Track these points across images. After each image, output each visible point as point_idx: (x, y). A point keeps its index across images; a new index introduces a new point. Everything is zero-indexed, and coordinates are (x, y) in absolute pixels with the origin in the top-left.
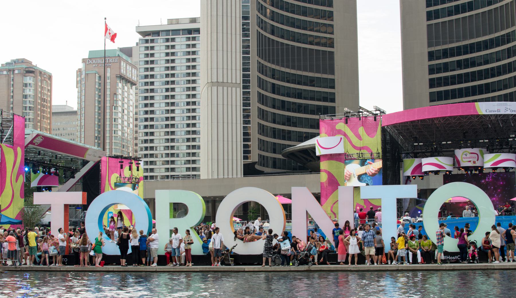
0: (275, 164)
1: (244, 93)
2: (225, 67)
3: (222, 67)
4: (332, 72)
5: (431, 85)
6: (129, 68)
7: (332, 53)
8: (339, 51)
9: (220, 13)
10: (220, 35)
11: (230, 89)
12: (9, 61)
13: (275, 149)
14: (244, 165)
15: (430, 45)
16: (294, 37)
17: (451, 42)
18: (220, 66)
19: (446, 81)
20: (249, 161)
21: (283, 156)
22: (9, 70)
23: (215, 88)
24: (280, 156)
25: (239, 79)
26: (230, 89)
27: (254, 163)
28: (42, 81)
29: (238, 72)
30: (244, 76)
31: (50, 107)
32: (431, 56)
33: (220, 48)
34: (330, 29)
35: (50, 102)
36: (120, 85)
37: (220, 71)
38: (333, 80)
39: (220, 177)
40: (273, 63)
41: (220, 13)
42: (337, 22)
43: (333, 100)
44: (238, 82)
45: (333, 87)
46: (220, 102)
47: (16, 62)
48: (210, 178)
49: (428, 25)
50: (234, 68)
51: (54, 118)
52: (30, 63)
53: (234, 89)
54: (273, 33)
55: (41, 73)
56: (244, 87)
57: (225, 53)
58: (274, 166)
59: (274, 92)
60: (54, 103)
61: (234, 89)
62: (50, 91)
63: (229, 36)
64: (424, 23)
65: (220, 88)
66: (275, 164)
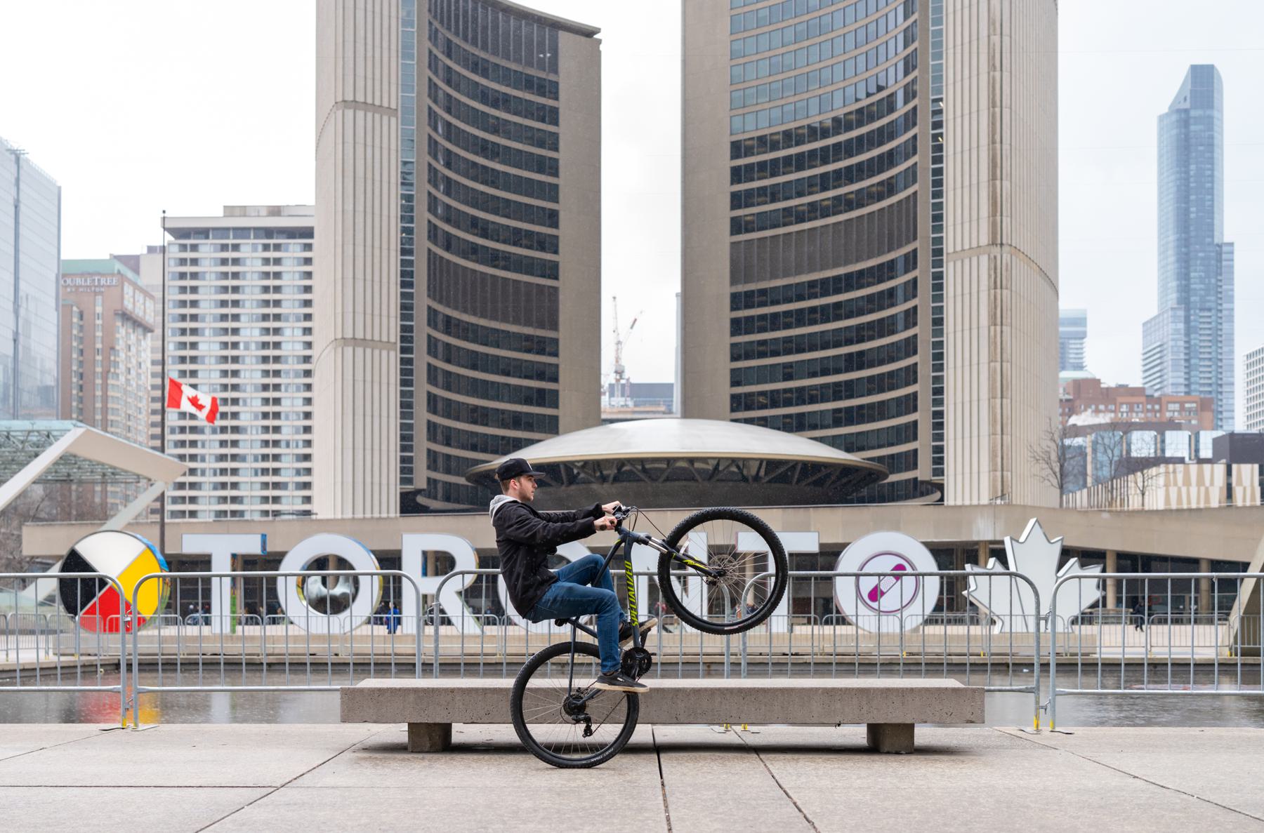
0: (451, 494)
1: (403, 361)
2: (369, 311)
4: (554, 326)
5: (734, 358)
6: (140, 297)
7: (556, 289)
8: (567, 285)
9: (360, 208)
10: (360, 250)
11: (377, 352)
13: (450, 465)
14: (401, 494)
15: (734, 282)
16: (494, 259)
17: (774, 276)
18: (360, 309)
19: (763, 350)
20: (409, 488)
21: (468, 479)
23: (349, 350)
24: (462, 481)
25: (395, 336)
26: (377, 352)
27: (419, 492)
29: (393, 320)
30: (405, 329)
32: (737, 301)
33: (360, 275)
34: (551, 244)
36: (122, 331)
37: (360, 319)
38: (555, 342)
39: (345, 516)
40: (448, 305)
41: (360, 208)
42: (565, 232)
43: (555, 379)
45: (555, 354)
46: (359, 377)
48: (339, 516)
49: (733, 244)
53: (384, 353)
54: (448, 248)
56: (403, 350)
58: (447, 499)
59: (448, 361)
61: (384, 353)
63: (377, 252)
64: (726, 239)
65: (360, 351)
66: (451, 494)
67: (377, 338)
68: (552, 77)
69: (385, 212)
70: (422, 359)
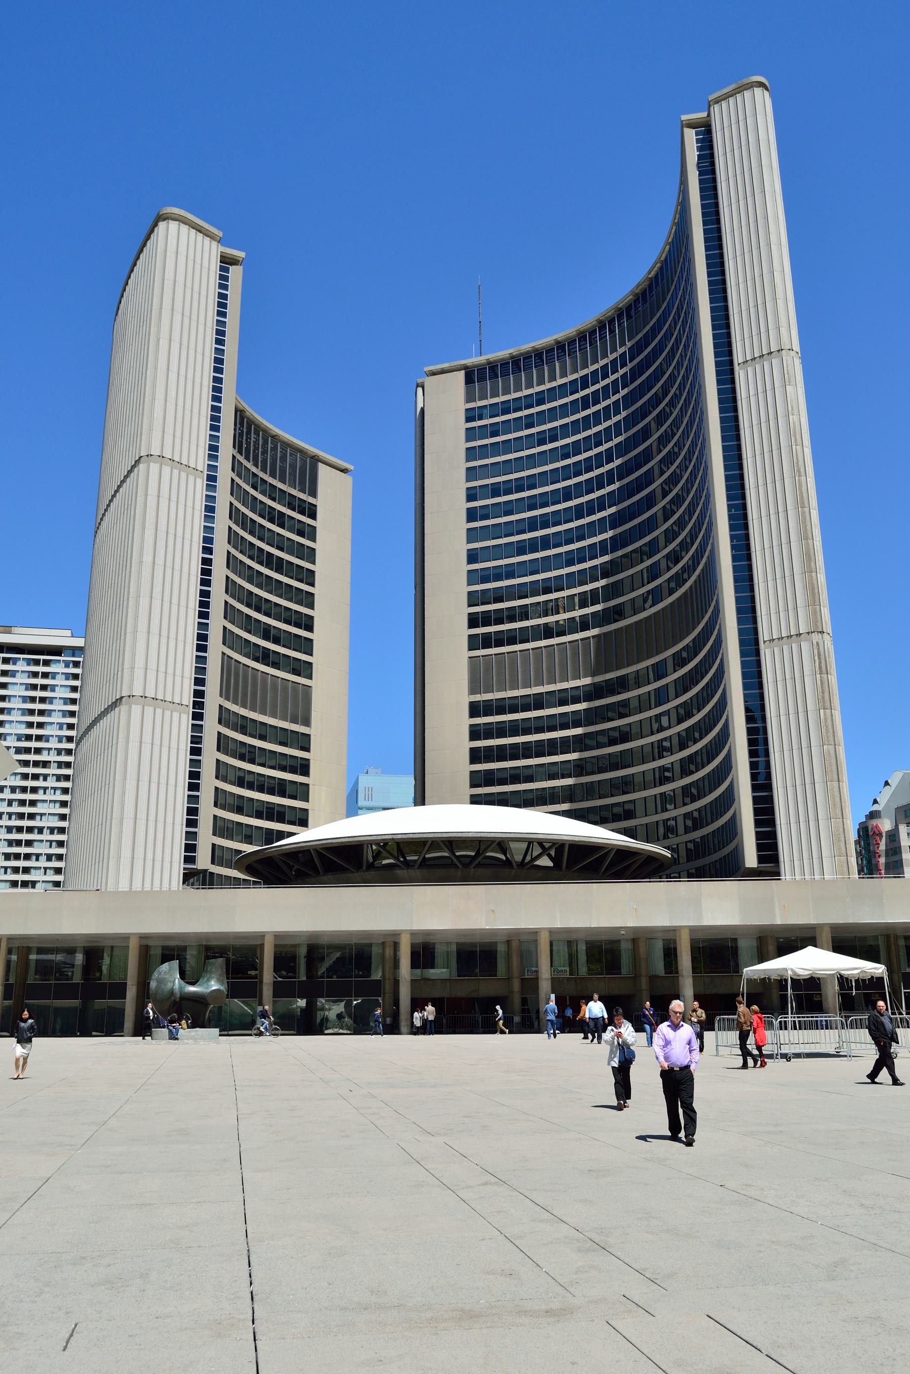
2: (162, 668)
3: (155, 668)
4: (307, 722)
9: (160, 561)
19: (501, 754)
25: (188, 699)
45: (307, 749)
50: (179, 672)
57: (164, 640)
65: (149, 710)
68: (311, 500)
69: (185, 569)
70: (211, 727)
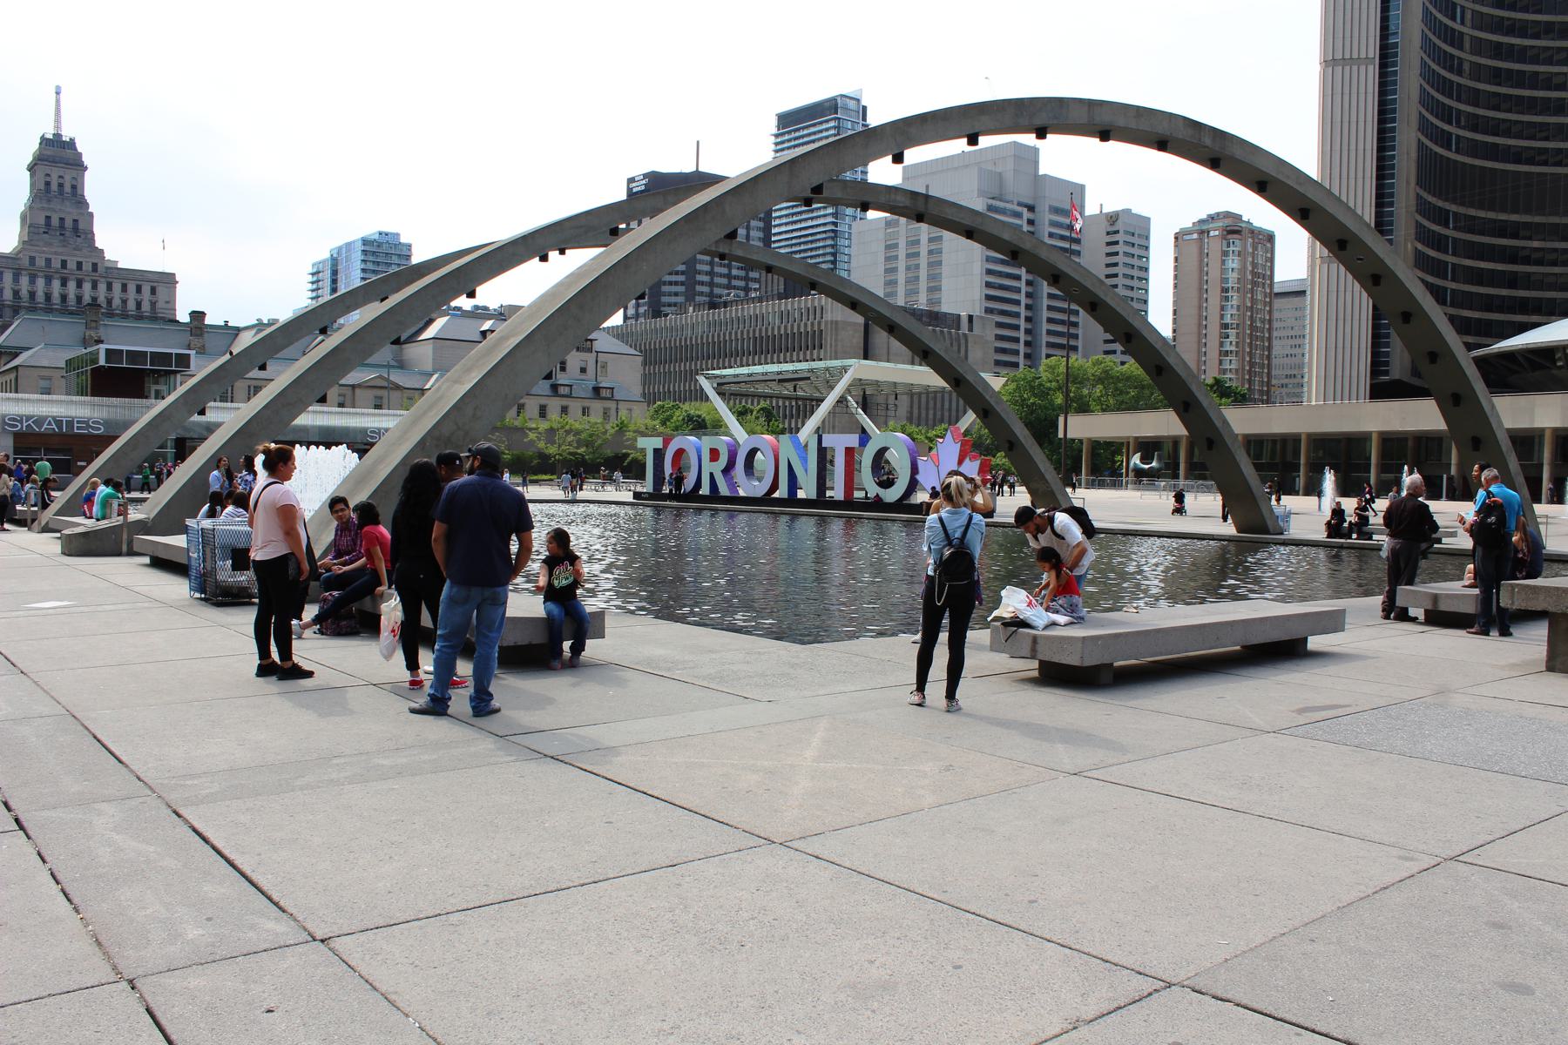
12: (1204, 216)
22: (1202, 232)
25: (1373, 51)
28: (1255, 248)
31: (1271, 285)
35: (1272, 276)
44: (1371, 55)
47: (1212, 218)
51: (1278, 303)
52: (1239, 217)
55: (1252, 232)
60: (1277, 279)
62: (1272, 260)
67: (1355, 56)
